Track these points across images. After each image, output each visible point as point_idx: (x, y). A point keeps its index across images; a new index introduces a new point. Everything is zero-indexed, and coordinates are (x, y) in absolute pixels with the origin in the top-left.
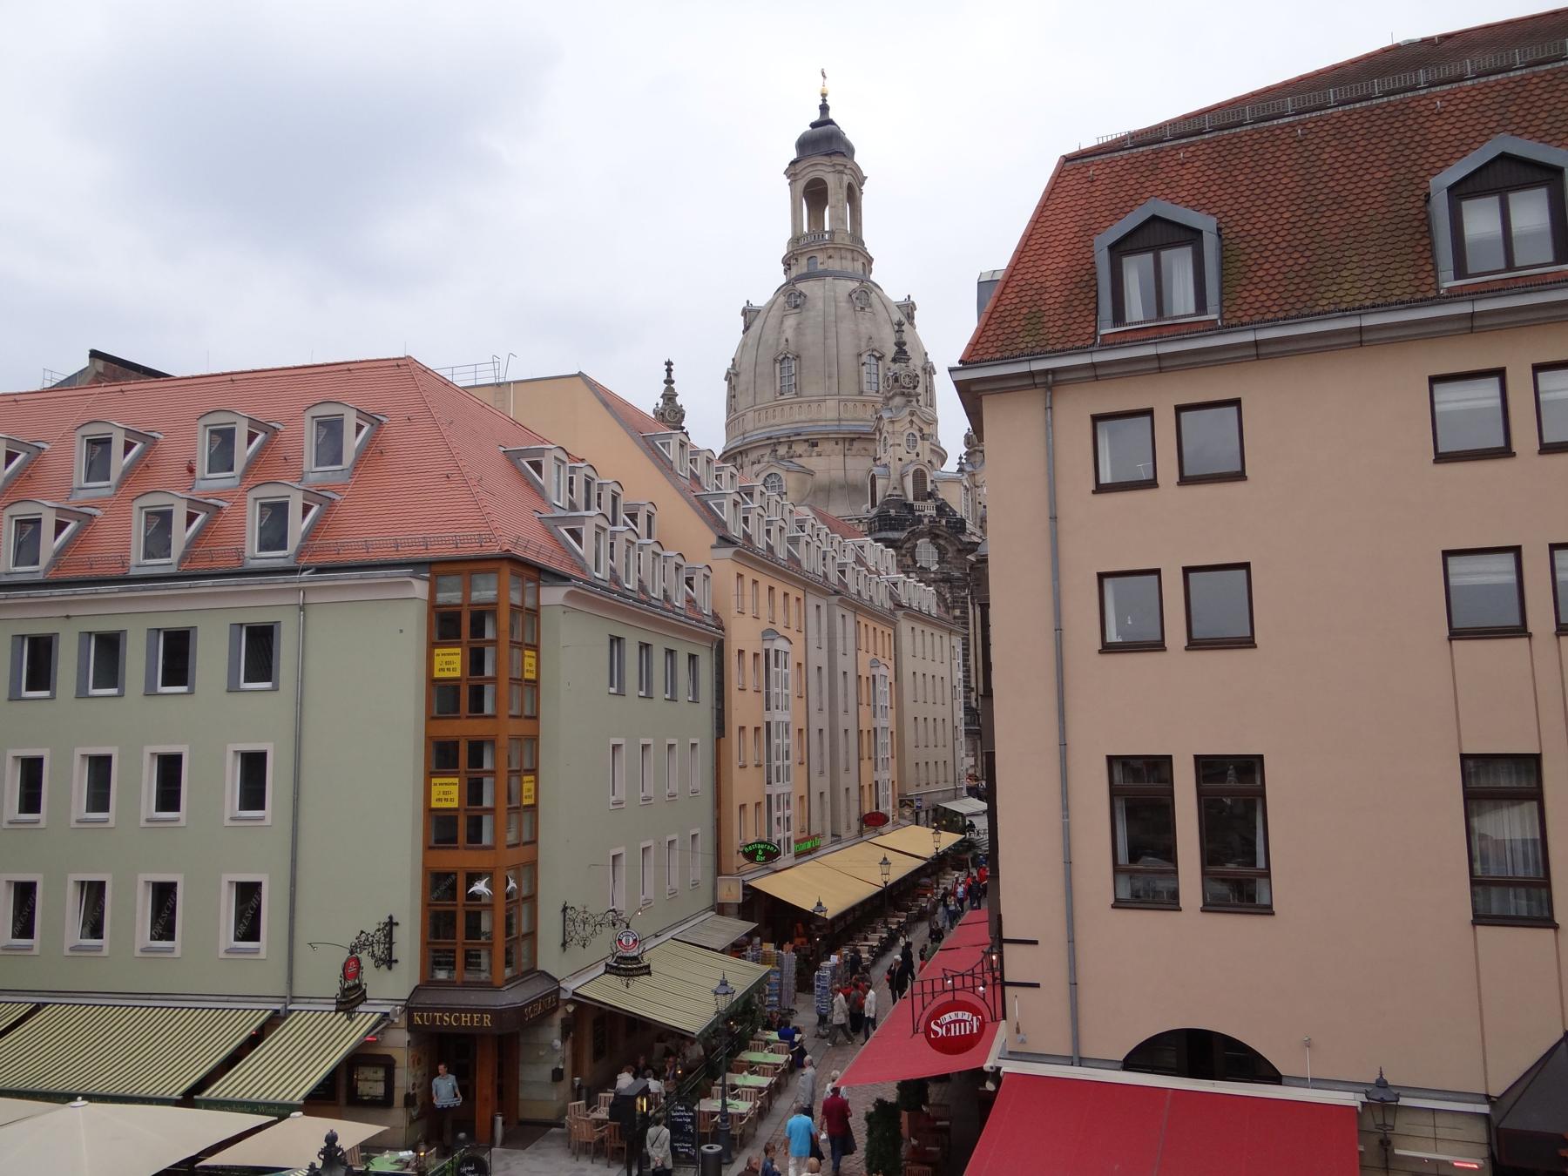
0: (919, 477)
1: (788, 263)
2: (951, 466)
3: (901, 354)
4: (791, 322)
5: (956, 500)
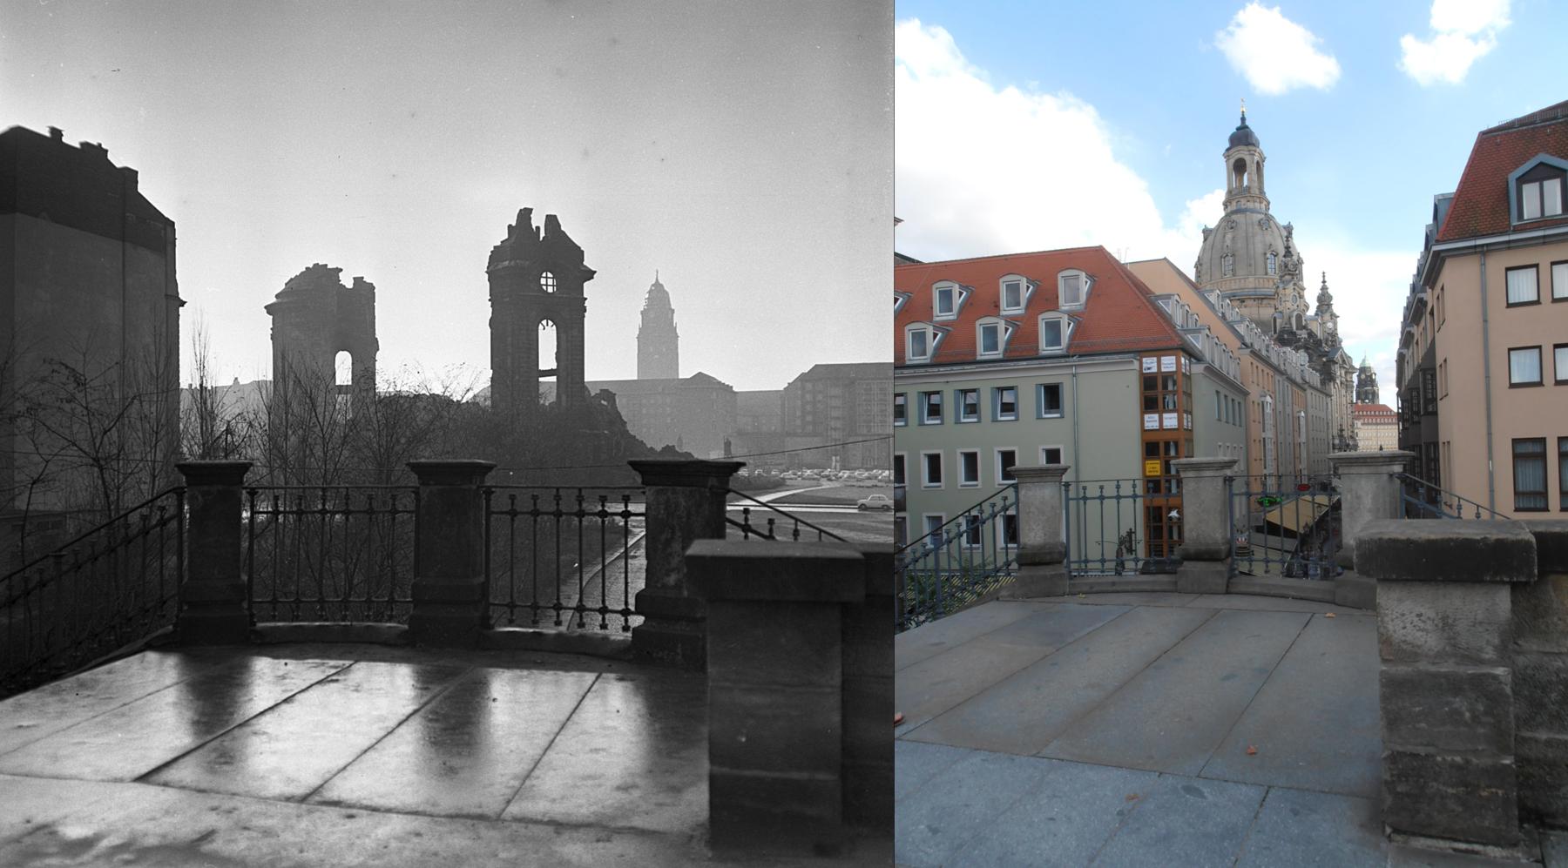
0: (1299, 317)
1: (1226, 205)
2: (1311, 312)
3: (1288, 251)
4: (1229, 236)
5: (1316, 328)
